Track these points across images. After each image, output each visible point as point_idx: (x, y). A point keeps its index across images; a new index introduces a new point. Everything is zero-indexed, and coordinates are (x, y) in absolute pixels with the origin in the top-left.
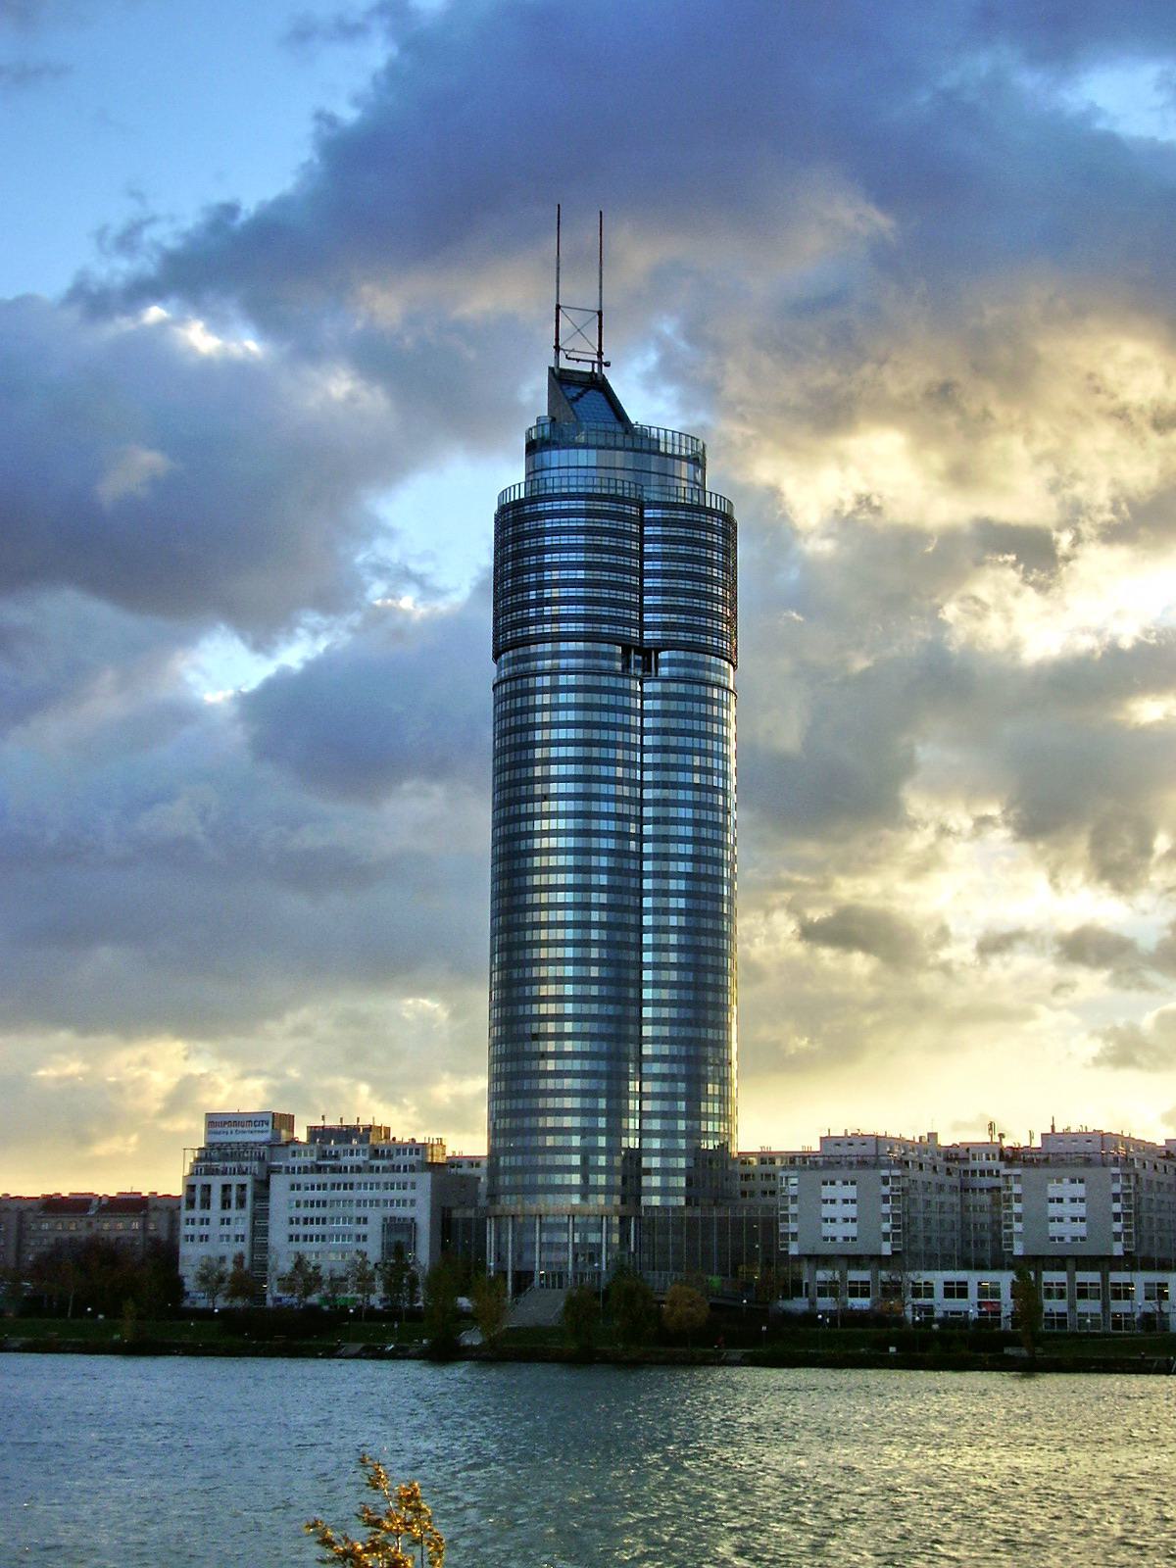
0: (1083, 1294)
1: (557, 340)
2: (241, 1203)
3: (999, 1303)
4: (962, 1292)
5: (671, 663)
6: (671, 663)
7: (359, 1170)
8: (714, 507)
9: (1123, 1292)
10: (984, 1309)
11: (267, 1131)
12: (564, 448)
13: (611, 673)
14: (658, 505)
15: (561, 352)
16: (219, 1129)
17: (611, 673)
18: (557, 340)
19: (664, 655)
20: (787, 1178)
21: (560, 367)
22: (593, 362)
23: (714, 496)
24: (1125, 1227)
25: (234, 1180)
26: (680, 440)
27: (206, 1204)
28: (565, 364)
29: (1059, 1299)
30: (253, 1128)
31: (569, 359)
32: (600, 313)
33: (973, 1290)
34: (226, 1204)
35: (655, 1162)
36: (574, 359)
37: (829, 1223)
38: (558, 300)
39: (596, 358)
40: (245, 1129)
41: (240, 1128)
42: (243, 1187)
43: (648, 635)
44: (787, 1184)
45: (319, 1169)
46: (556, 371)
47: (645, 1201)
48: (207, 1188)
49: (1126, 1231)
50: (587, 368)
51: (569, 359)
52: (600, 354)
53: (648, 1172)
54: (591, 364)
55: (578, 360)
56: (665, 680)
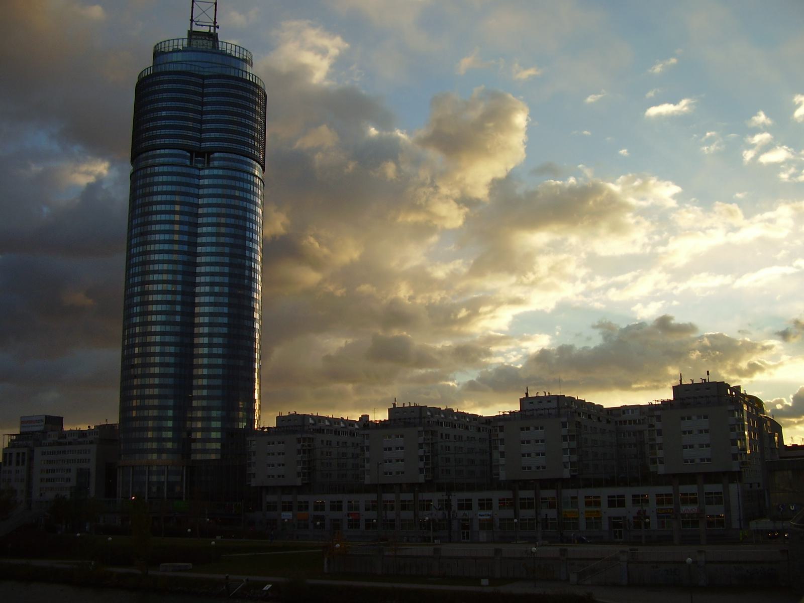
0: (404, 508)
1: (192, 17)
3: (358, 514)
4: (340, 508)
7: (70, 443)
8: (251, 80)
9: (427, 506)
10: (351, 518)
11: (42, 425)
13: (187, 166)
17: (187, 166)
18: (192, 17)
20: (251, 441)
22: (210, 26)
24: (426, 464)
26: (239, 50)
27: (10, 463)
28: (196, 28)
29: (392, 510)
30: (37, 424)
32: (216, 4)
33: (345, 505)
34: (18, 463)
35: (199, 435)
36: (200, 25)
37: (271, 467)
39: (213, 25)
40: (35, 424)
42: (24, 454)
44: (251, 445)
45: (60, 444)
47: (193, 457)
48: (11, 454)
49: (426, 467)
50: (206, 29)
51: (197, 25)
52: (215, 22)
53: (195, 440)
54: (209, 27)
55: (202, 26)
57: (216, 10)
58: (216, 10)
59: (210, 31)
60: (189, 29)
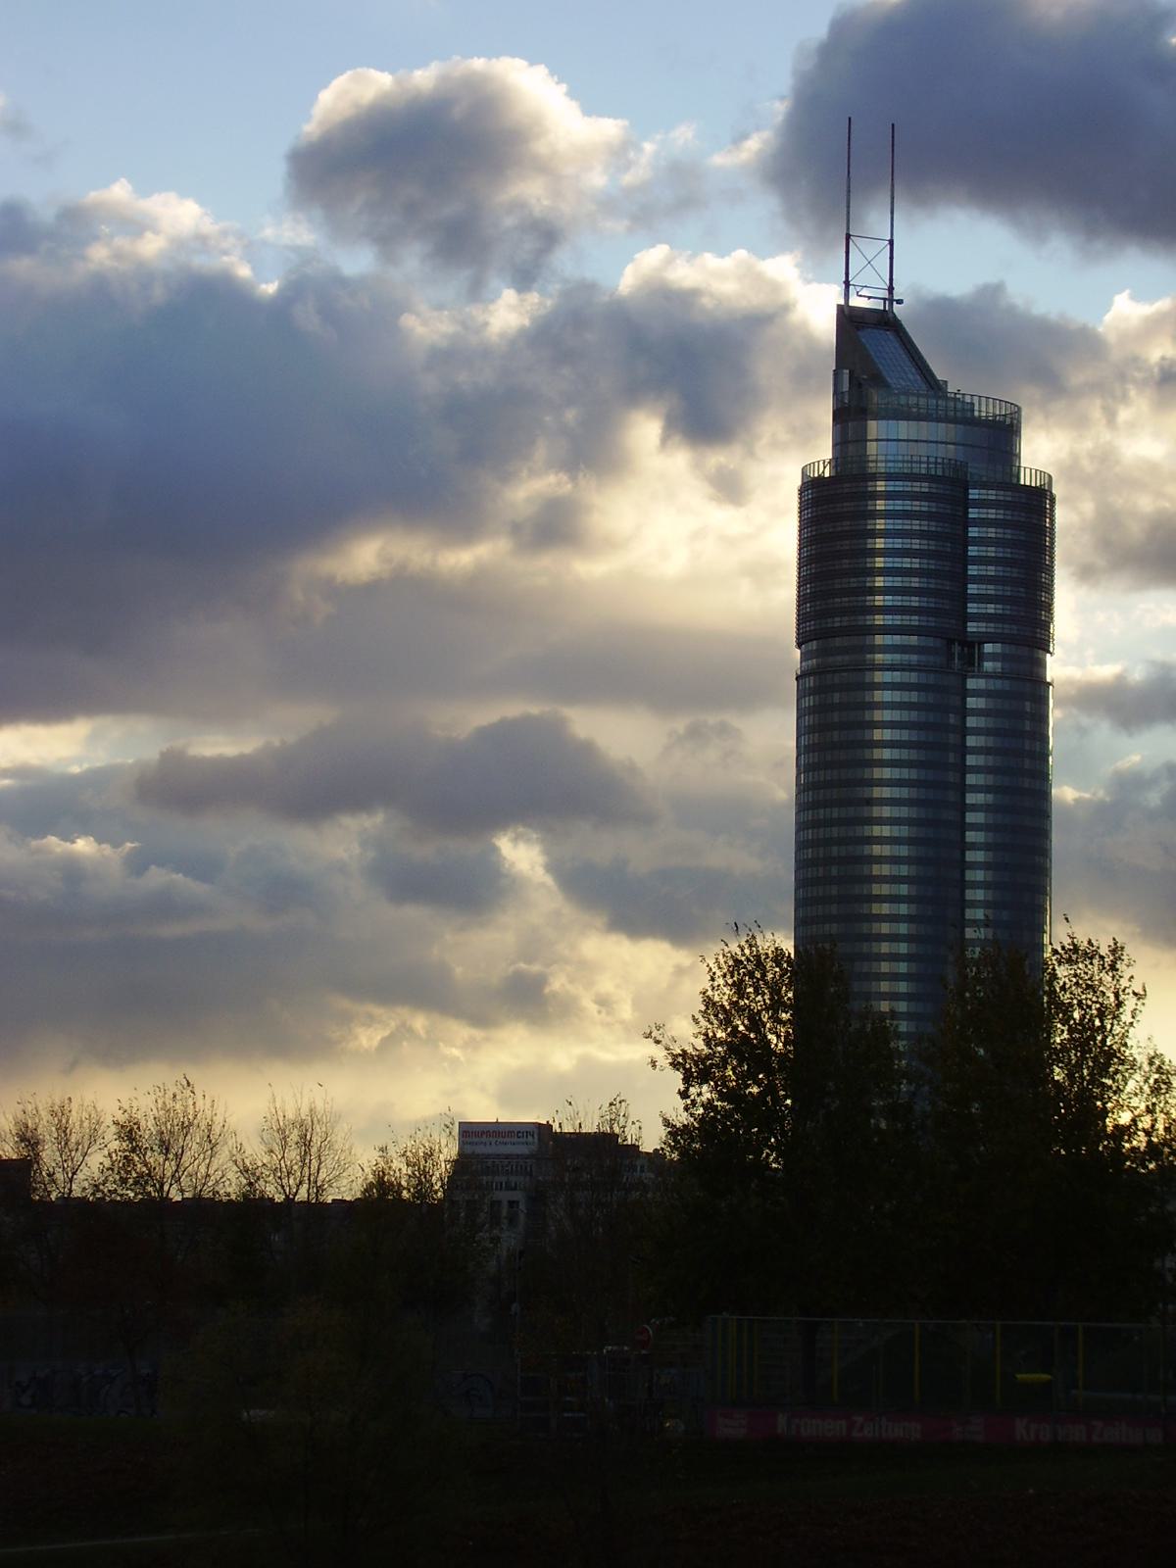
2: (512, 1220)
5: (994, 657)
6: (994, 657)
12: (883, 418)
14: (984, 486)
15: (851, 287)
16: (476, 1140)
19: (988, 648)
21: (850, 304)
22: (885, 299)
23: (1038, 473)
25: (504, 1196)
28: (855, 302)
30: (516, 1140)
31: (861, 296)
32: (891, 242)
36: (865, 296)
38: (848, 228)
39: (885, 294)
41: (500, 1140)
42: (512, 1204)
43: (972, 627)
46: (846, 310)
50: (879, 305)
51: (861, 296)
52: (891, 289)
56: (988, 676)
57: (891, 258)
58: (891, 258)
59: (885, 307)
60: (842, 302)
